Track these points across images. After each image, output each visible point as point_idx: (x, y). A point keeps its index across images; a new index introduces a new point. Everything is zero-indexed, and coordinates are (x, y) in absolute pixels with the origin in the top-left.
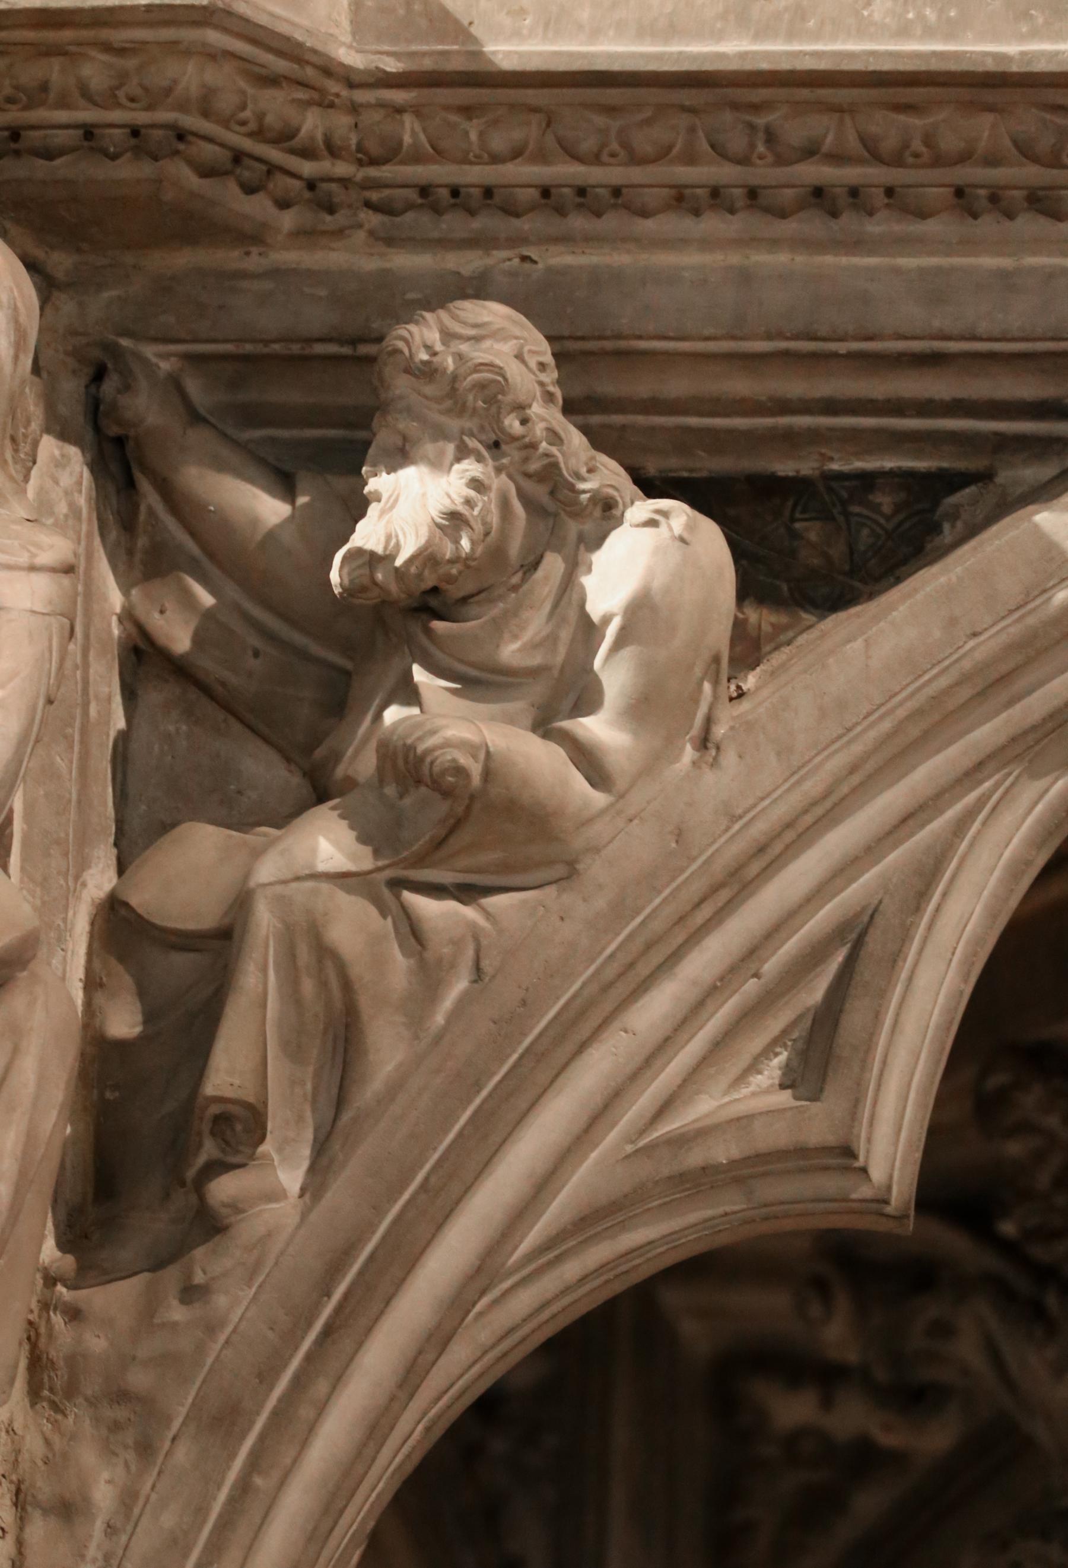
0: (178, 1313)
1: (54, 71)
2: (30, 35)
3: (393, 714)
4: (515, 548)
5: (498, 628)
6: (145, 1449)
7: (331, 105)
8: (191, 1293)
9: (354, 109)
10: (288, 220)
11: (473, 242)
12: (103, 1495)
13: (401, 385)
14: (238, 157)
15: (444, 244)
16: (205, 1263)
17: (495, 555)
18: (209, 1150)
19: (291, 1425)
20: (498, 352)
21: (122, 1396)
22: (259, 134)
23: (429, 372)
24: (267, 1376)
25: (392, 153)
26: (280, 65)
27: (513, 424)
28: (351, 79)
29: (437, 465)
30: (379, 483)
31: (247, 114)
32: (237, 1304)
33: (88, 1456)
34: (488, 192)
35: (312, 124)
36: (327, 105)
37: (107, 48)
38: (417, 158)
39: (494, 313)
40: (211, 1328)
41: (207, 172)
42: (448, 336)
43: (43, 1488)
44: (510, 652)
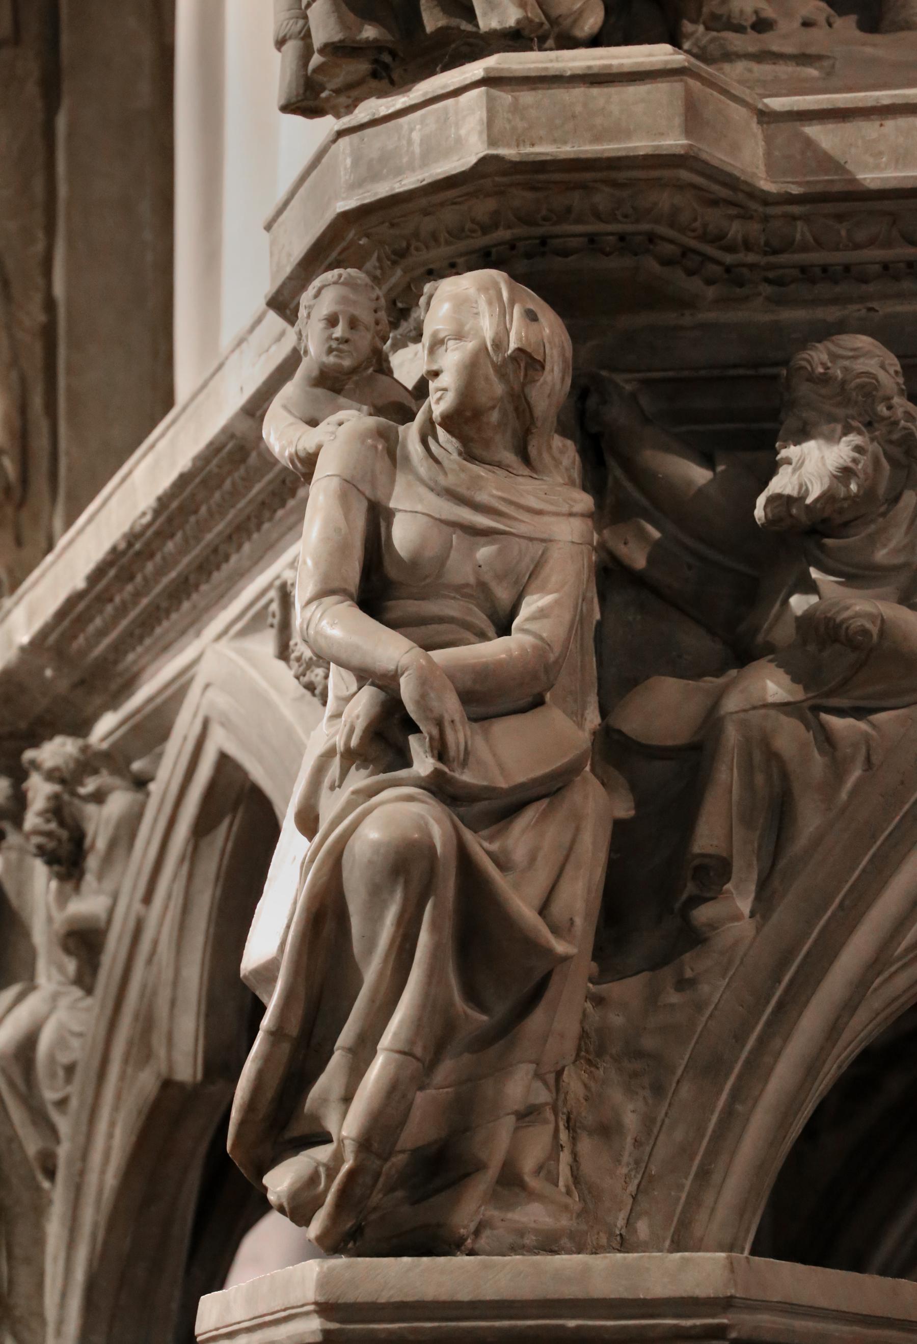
0: (674, 998)
1: (576, 199)
2: (565, 177)
3: (799, 603)
4: (882, 489)
5: (872, 541)
6: (658, 1090)
7: (751, 218)
8: (682, 984)
9: (766, 219)
10: (711, 292)
11: (835, 301)
12: (631, 1120)
13: (804, 389)
14: (686, 251)
15: (815, 302)
16: (692, 964)
17: (869, 494)
18: (690, 889)
19: (757, 1069)
20: (869, 365)
21: (639, 1054)
22: (704, 237)
23: (825, 379)
24: (740, 1038)
25: (788, 246)
26: (724, 193)
27: (882, 409)
28: (766, 199)
29: (831, 439)
30: (791, 452)
31: (697, 224)
32: (717, 990)
33: (616, 1095)
34: (847, 268)
35: (736, 230)
36: (746, 216)
37: (615, 184)
38: (805, 248)
39: (864, 341)
40: (699, 1007)
41: (667, 262)
42: (834, 357)
43: (588, 1118)
44: (881, 555)
